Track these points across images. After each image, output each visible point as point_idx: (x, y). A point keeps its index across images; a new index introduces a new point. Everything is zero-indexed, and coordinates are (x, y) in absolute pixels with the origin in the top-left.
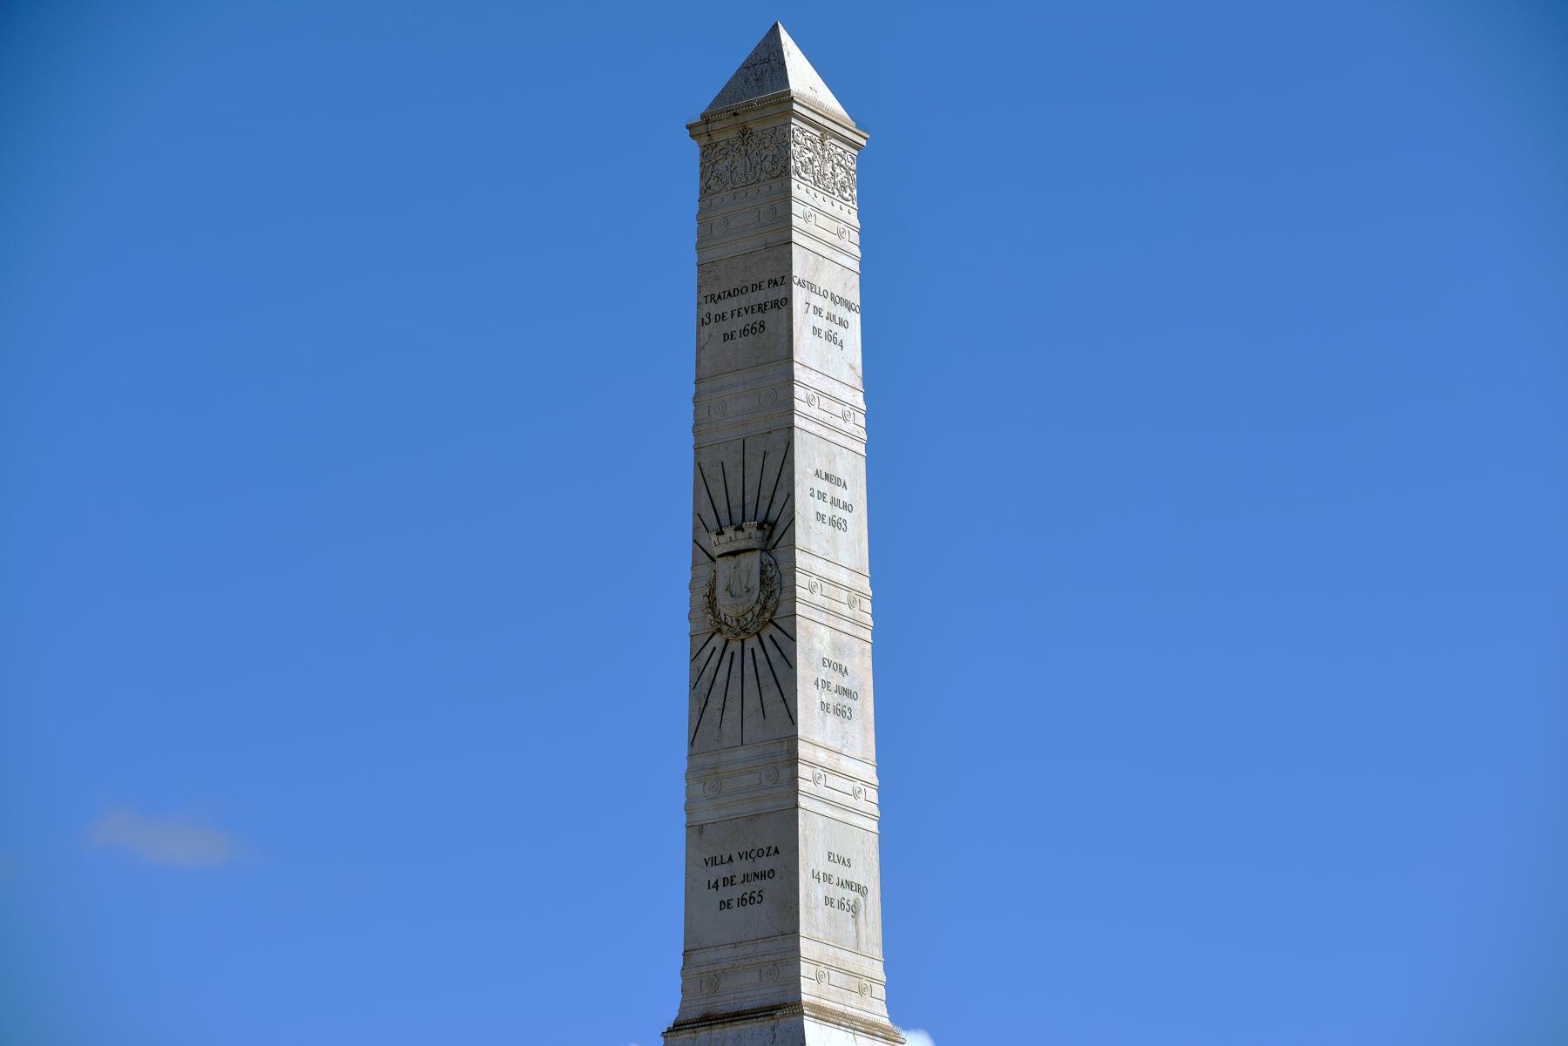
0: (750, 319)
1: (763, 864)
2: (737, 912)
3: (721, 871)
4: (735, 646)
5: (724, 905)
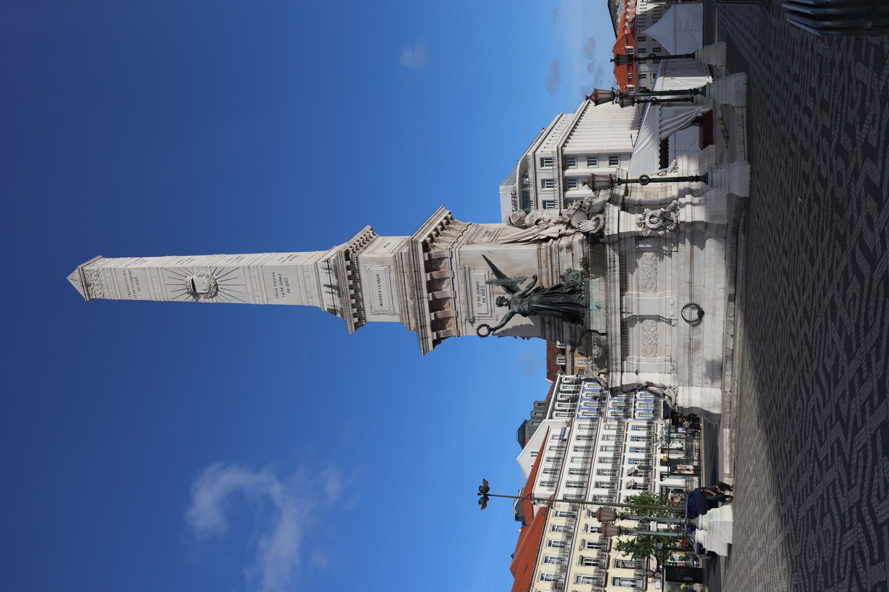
0: (134, 282)
1: (277, 278)
3: (280, 292)
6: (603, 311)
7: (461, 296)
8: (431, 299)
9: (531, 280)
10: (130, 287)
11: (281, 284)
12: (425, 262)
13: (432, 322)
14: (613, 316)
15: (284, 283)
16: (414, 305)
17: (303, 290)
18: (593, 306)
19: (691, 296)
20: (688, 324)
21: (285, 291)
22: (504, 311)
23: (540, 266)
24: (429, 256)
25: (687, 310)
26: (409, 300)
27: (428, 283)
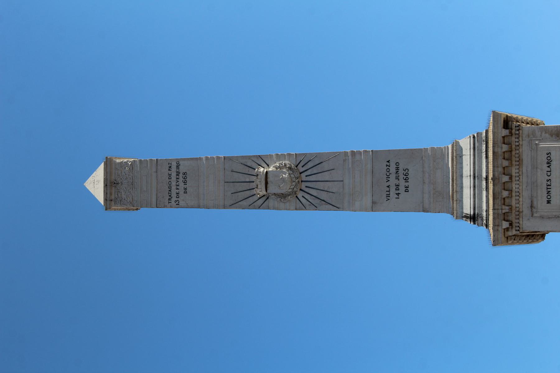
0: (181, 179)
1: (393, 169)
2: (411, 183)
4: (303, 186)
5: (407, 189)
10: (174, 187)
11: (397, 178)
15: (401, 176)
21: (402, 189)
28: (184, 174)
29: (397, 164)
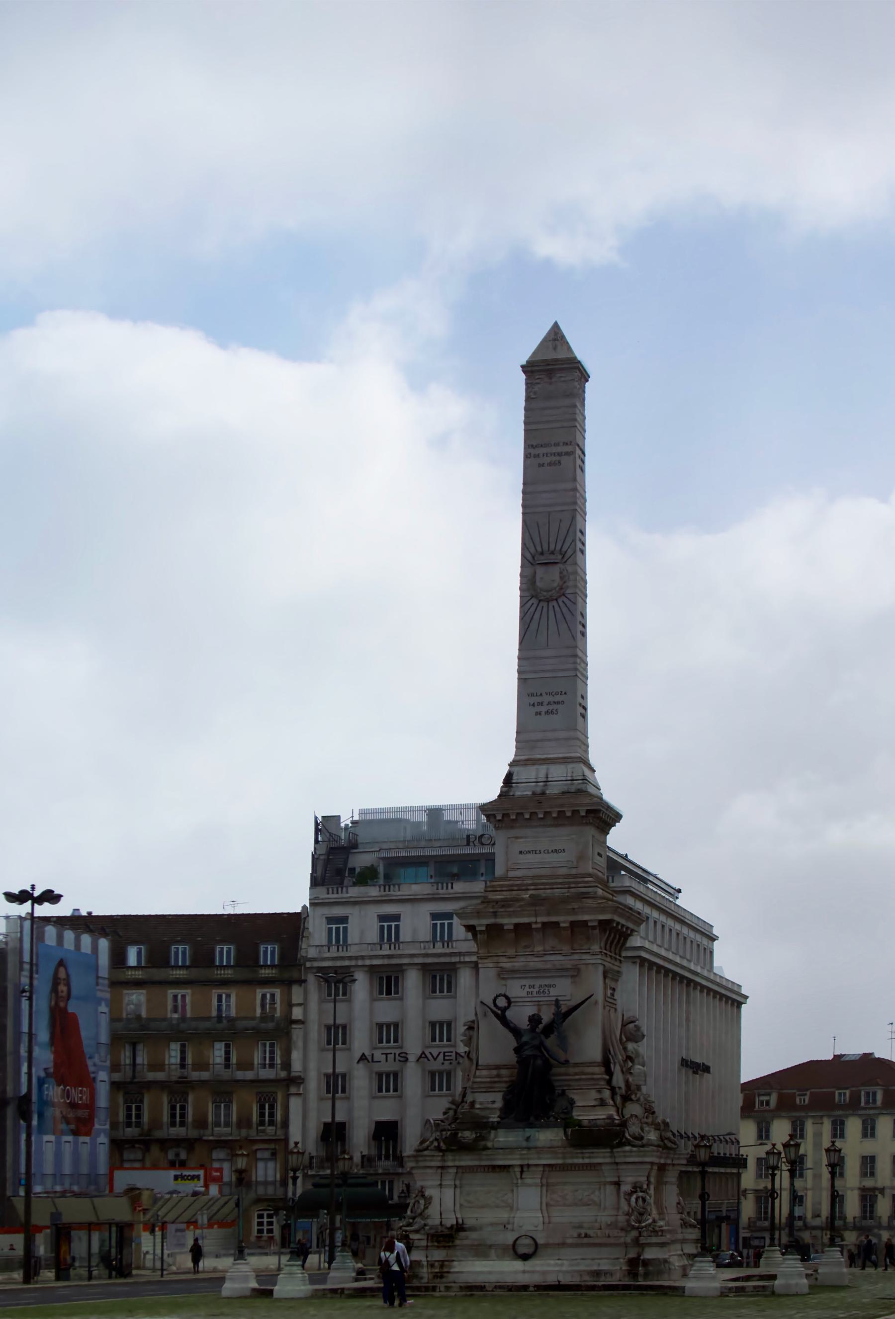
1: (558, 698)
5: (538, 713)
6: (524, 1144)
7: (535, 963)
8: (534, 926)
9: (562, 1059)
12: (586, 922)
13: (502, 925)
14: (518, 1157)
15: (550, 707)
16: (523, 899)
17: (539, 736)
18: (529, 1132)
19: (547, 1245)
20: (511, 1242)
22: (523, 1023)
23: (576, 1065)
24: (594, 928)
25: (528, 1241)
26: (531, 892)
27: (557, 924)
28: (559, 462)
29: (563, 702)
